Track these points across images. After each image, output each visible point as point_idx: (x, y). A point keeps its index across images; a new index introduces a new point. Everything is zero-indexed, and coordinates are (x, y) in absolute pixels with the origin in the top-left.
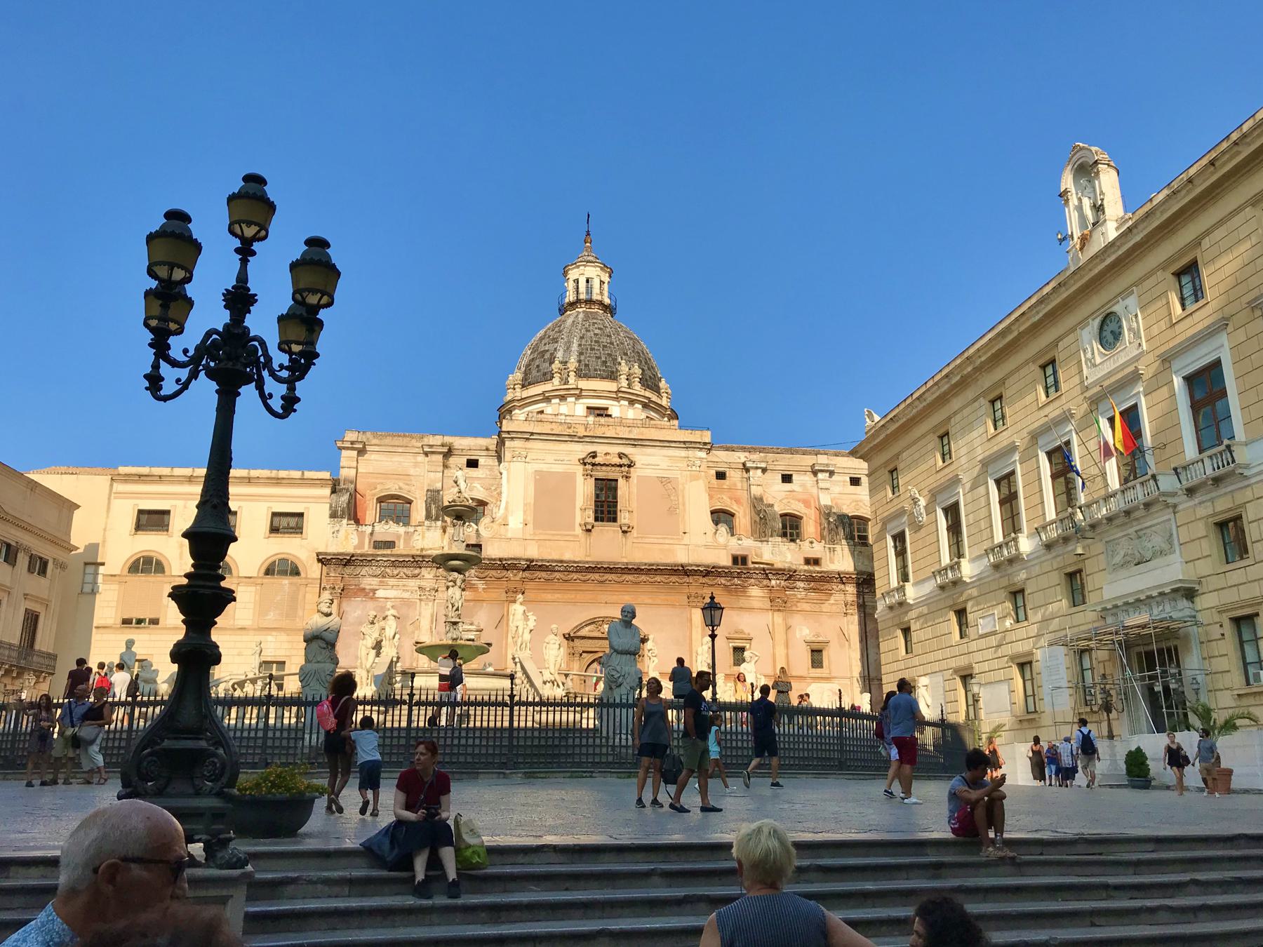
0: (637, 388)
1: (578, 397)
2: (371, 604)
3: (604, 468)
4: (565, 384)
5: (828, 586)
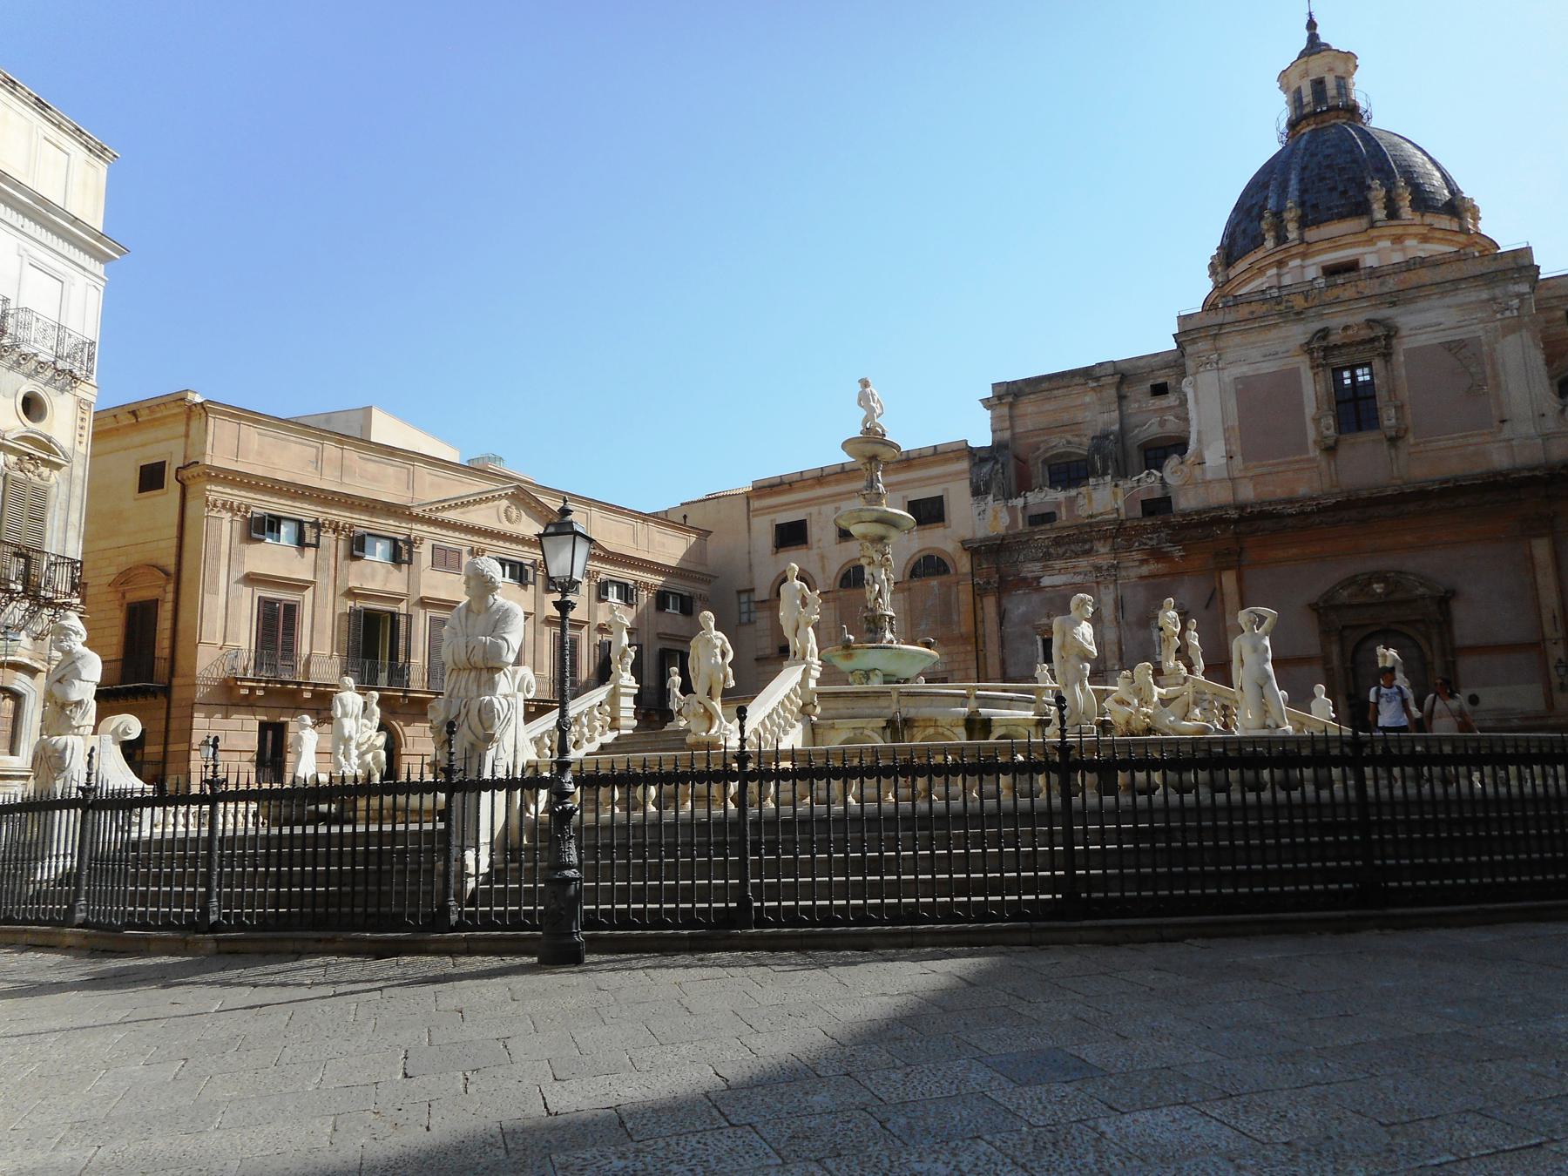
1: (1304, 256)
2: (1036, 598)
3: (1344, 351)
4: (1285, 242)
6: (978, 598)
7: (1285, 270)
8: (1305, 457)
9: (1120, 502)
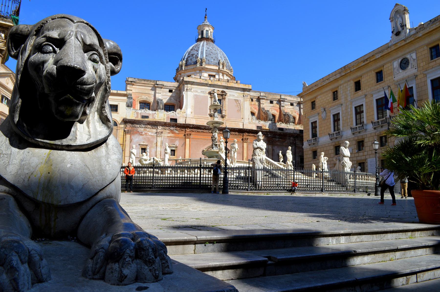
2: (141, 137)
7: (200, 72)
8: (207, 116)
9: (165, 118)
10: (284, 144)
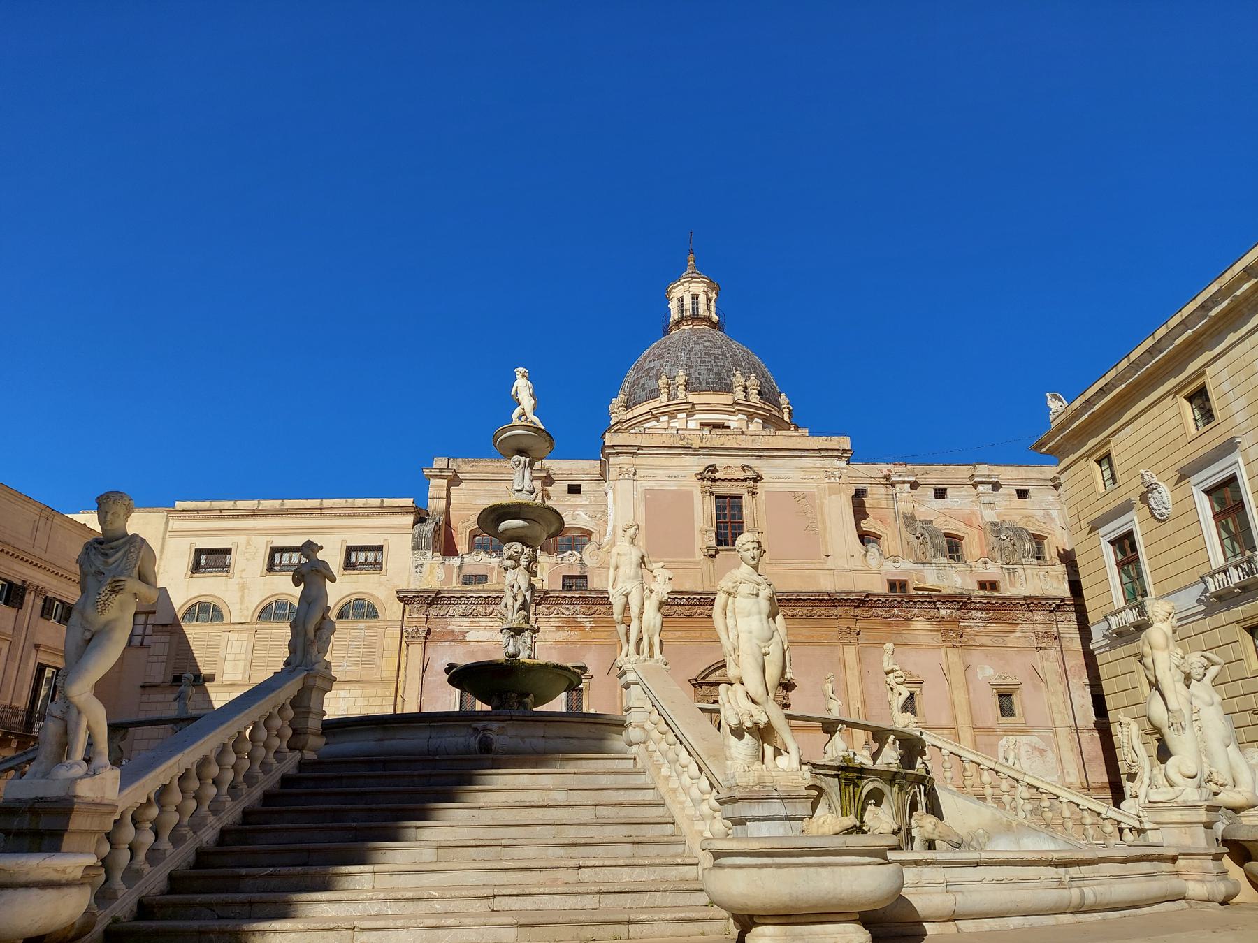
0: (755, 399)
3: (725, 484)
4: (674, 399)
5: (1011, 615)
6: (404, 645)
10: (1011, 641)
